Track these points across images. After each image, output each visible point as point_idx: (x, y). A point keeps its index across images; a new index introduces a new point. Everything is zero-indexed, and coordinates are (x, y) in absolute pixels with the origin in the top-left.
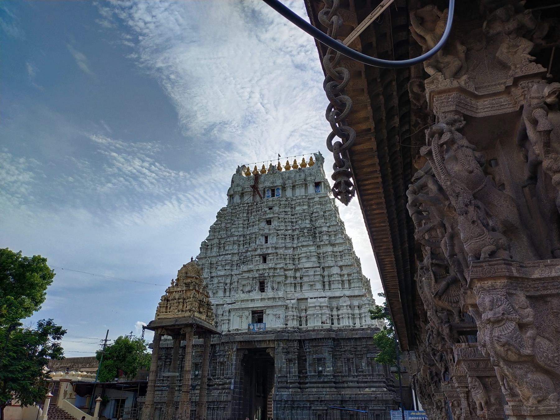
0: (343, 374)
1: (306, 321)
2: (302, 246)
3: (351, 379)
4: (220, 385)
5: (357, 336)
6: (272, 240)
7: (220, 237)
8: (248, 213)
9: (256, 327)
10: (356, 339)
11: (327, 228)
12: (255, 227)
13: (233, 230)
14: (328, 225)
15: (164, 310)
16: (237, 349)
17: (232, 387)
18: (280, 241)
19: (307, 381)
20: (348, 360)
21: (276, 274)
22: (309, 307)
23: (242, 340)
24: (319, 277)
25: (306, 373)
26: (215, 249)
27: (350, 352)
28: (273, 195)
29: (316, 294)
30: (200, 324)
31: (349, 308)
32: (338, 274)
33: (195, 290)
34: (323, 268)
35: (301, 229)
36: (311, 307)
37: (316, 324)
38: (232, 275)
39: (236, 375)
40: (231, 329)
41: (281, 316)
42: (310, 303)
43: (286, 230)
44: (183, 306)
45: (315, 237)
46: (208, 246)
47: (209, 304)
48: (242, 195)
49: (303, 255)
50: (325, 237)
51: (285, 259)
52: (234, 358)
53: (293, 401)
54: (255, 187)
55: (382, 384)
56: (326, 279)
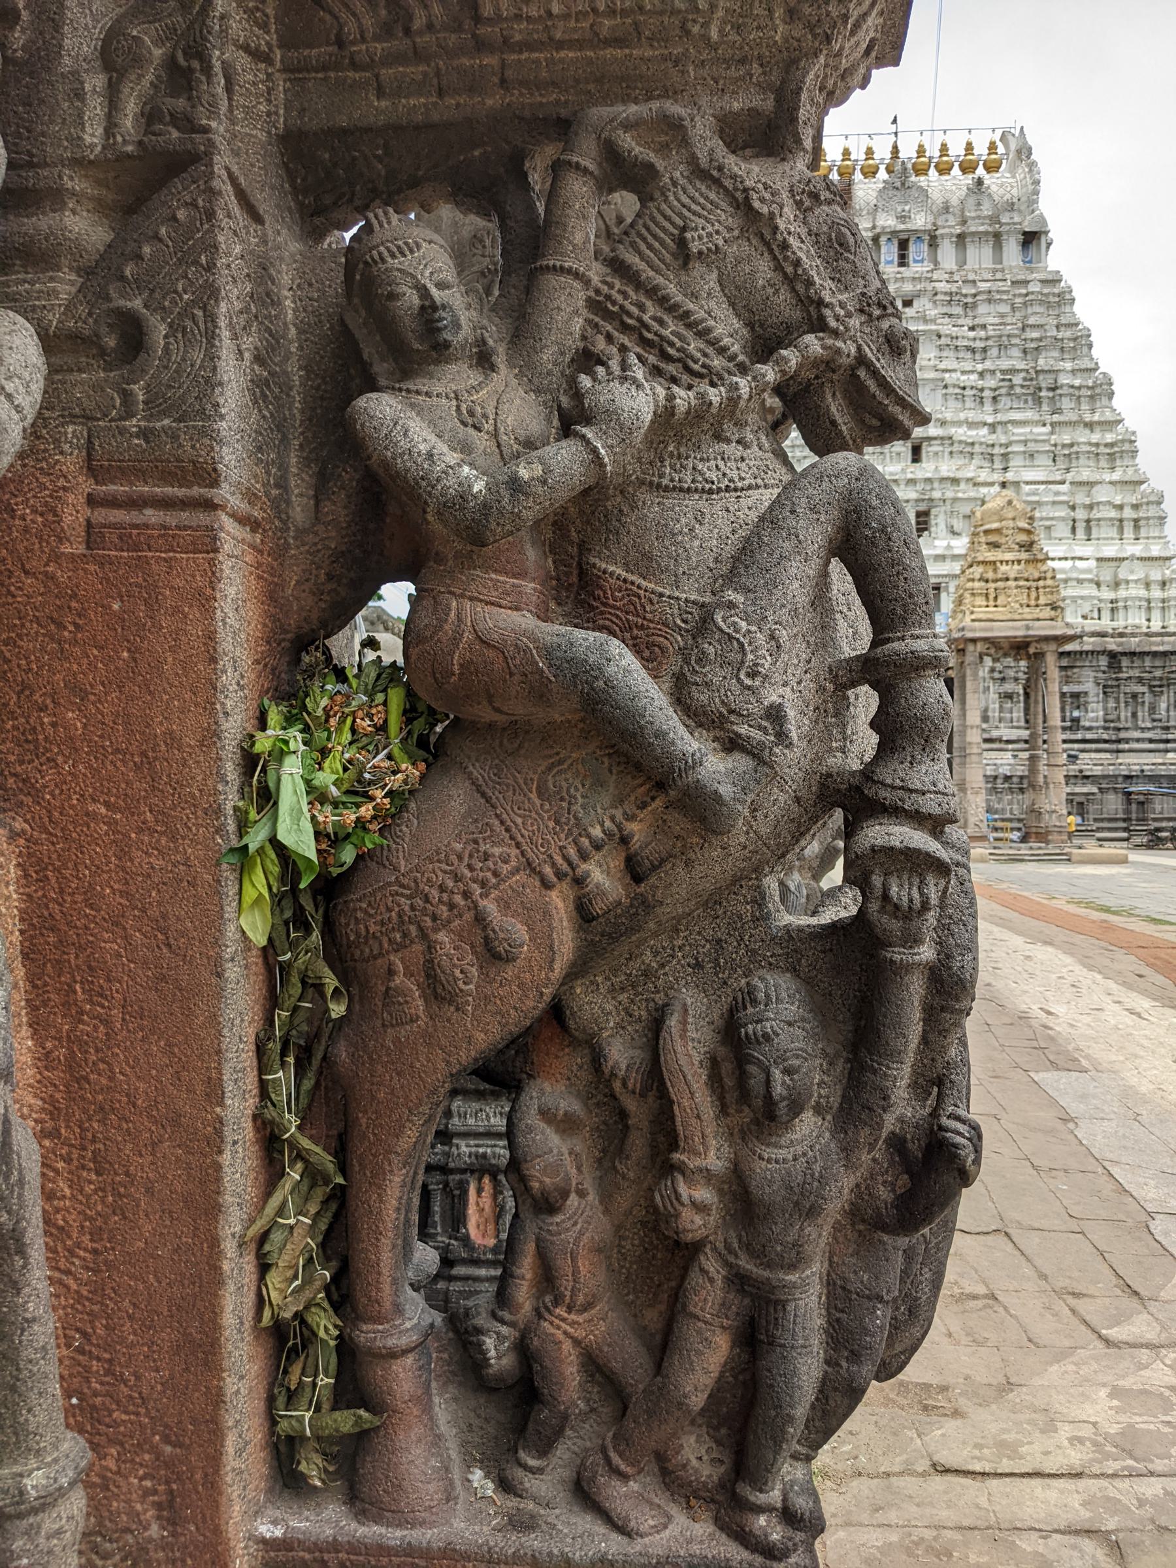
3: (1137, 734)
5: (1161, 649)
10: (1155, 654)
14: (1068, 365)
18: (952, 403)
20: (1134, 696)
21: (960, 495)
27: (1140, 680)
28: (903, 261)
32: (1109, 503)
43: (963, 373)
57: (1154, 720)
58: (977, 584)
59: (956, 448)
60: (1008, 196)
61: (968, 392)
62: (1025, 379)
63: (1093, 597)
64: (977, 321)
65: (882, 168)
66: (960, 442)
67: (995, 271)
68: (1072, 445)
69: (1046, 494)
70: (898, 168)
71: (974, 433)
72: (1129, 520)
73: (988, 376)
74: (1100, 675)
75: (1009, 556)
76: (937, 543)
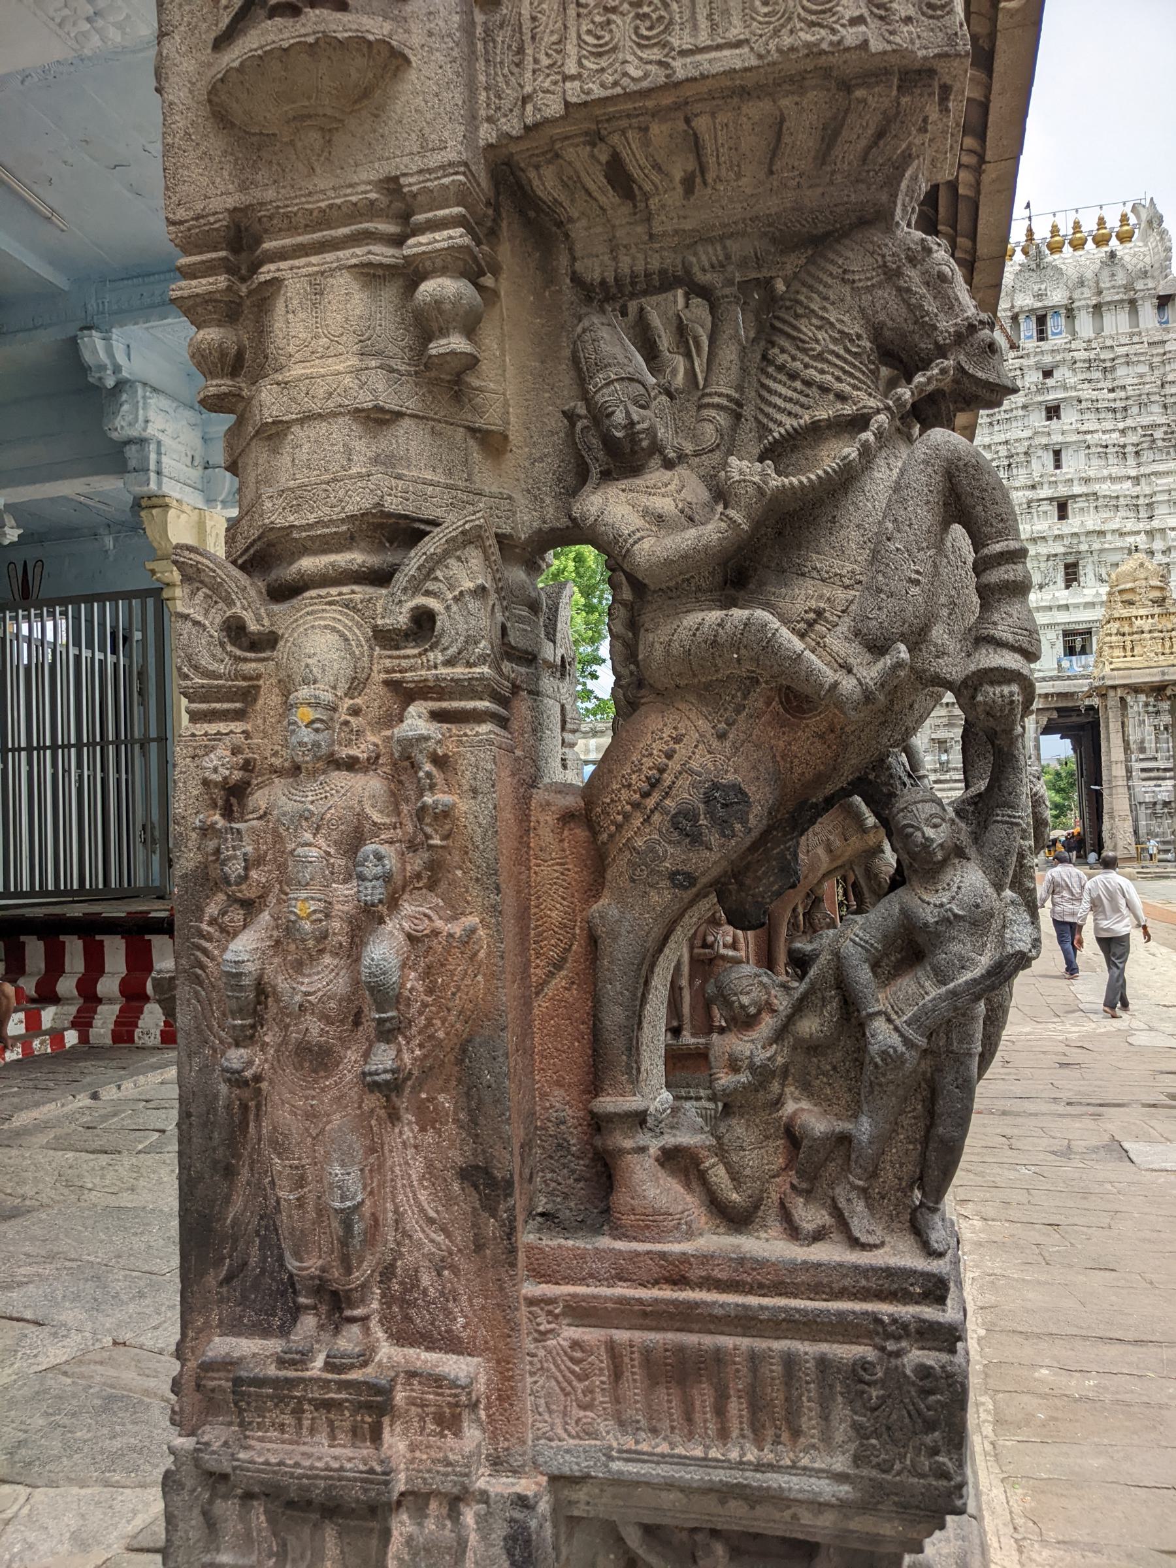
6: (1073, 464)
12: (1014, 424)
18: (1095, 462)
28: (1042, 335)
43: (1104, 432)
49: (1159, 498)
59: (1101, 502)
60: (1141, 265)
61: (1111, 450)
62: (1166, 433)
64: (1116, 383)
65: (1018, 250)
66: (1105, 497)
67: (1132, 335)
70: (1033, 251)
71: (1117, 487)
73: (1130, 433)
75: (1142, 612)
76: (1086, 591)
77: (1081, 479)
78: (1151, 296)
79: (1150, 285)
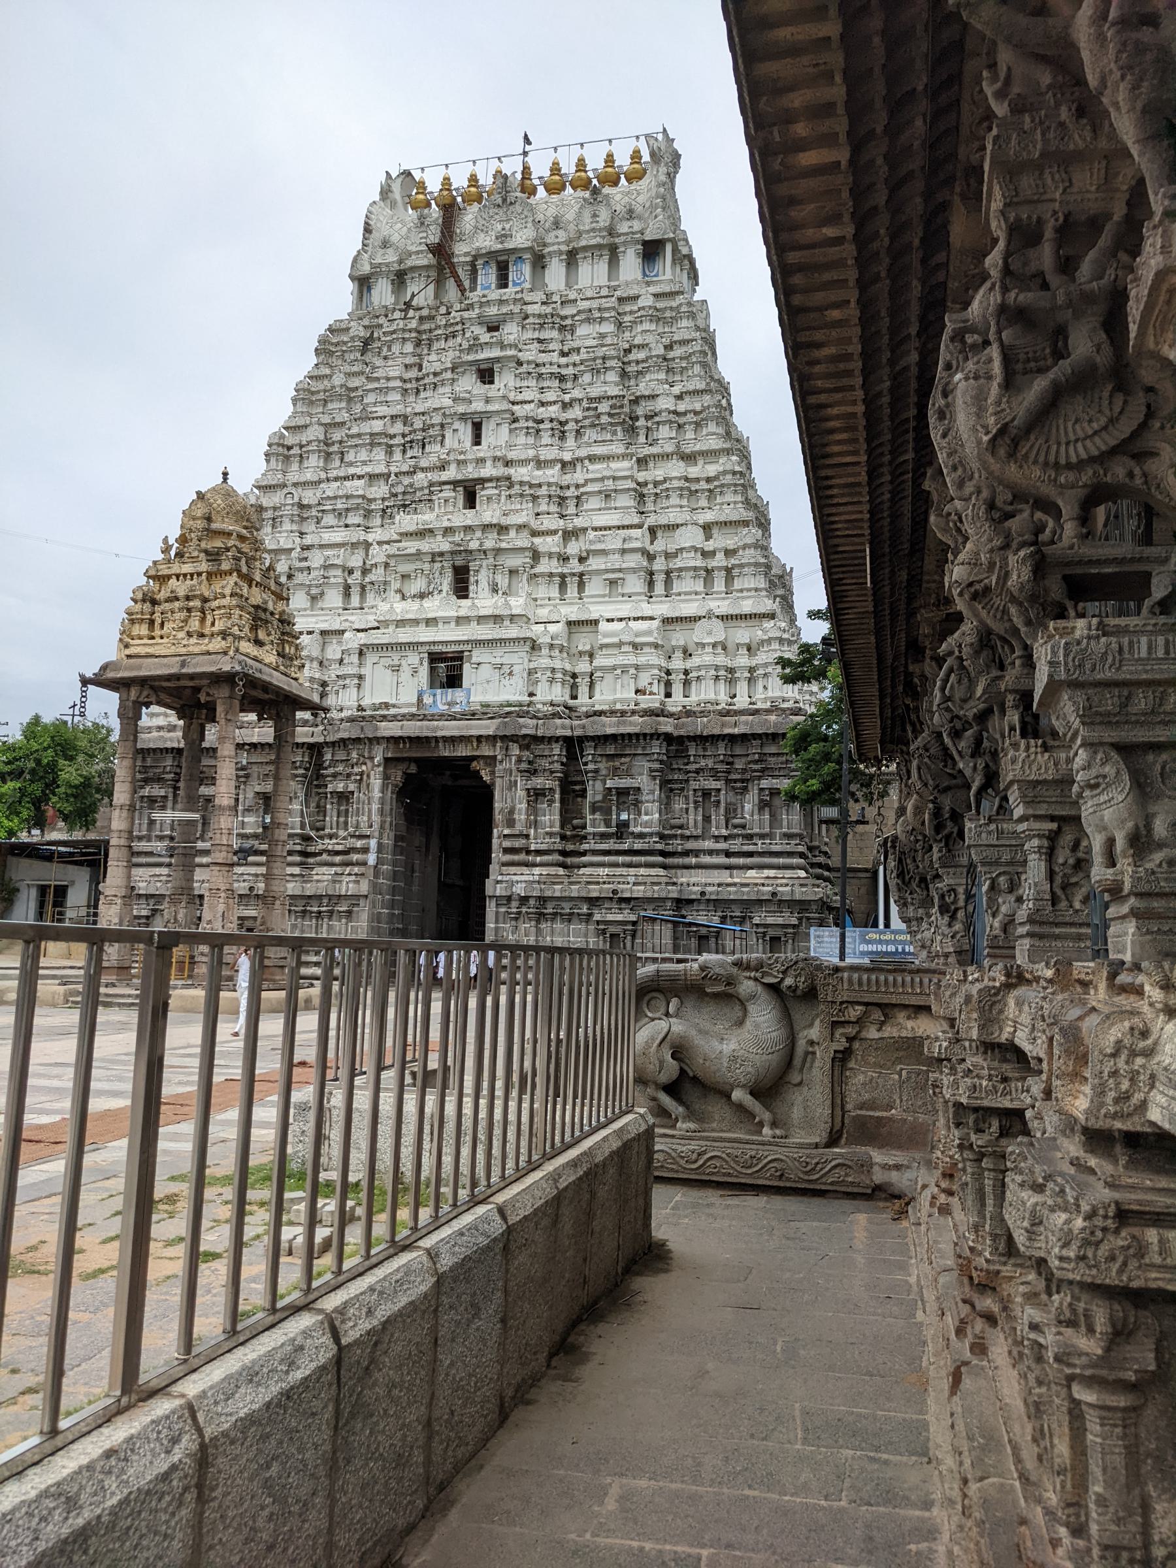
0: (687, 833)
1: (591, 686)
2: (592, 459)
3: (708, 844)
4: (337, 853)
5: (736, 731)
6: (496, 437)
7: (326, 419)
8: (418, 344)
9: (440, 700)
10: (732, 739)
11: (672, 400)
12: (441, 390)
13: (370, 398)
14: (677, 390)
15: (144, 630)
16: (387, 760)
17: (372, 859)
18: (522, 439)
19: (585, 847)
20: (706, 794)
21: (504, 545)
22: (602, 647)
23: (398, 733)
24: (638, 557)
25: (584, 827)
26: (314, 461)
28: (503, 282)
29: (625, 609)
30: (258, 675)
31: (719, 650)
32: (696, 550)
33: (239, 571)
34: (653, 531)
35: (590, 400)
36: (607, 646)
37: (618, 696)
38: (367, 545)
39: (382, 827)
40: (366, 702)
41: (516, 669)
42: (605, 635)
43: (542, 404)
44: (203, 620)
45: (632, 431)
46: (289, 448)
47: (286, 621)
48: (400, 278)
49: (590, 488)
50: (664, 432)
51: (535, 498)
52: (376, 783)
53: (543, 900)
54: (441, 252)
55: (796, 861)
56: (659, 565)
57: (735, 827)
58: (138, 607)
59: (516, 489)
63: (652, 666)
66: (521, 483)
68: (665, 481)
69: (613, 542)
72: (720, 568)
74: (657, 766)
77: (495, 459)
78: (637, 242)
79: (637, 225)
